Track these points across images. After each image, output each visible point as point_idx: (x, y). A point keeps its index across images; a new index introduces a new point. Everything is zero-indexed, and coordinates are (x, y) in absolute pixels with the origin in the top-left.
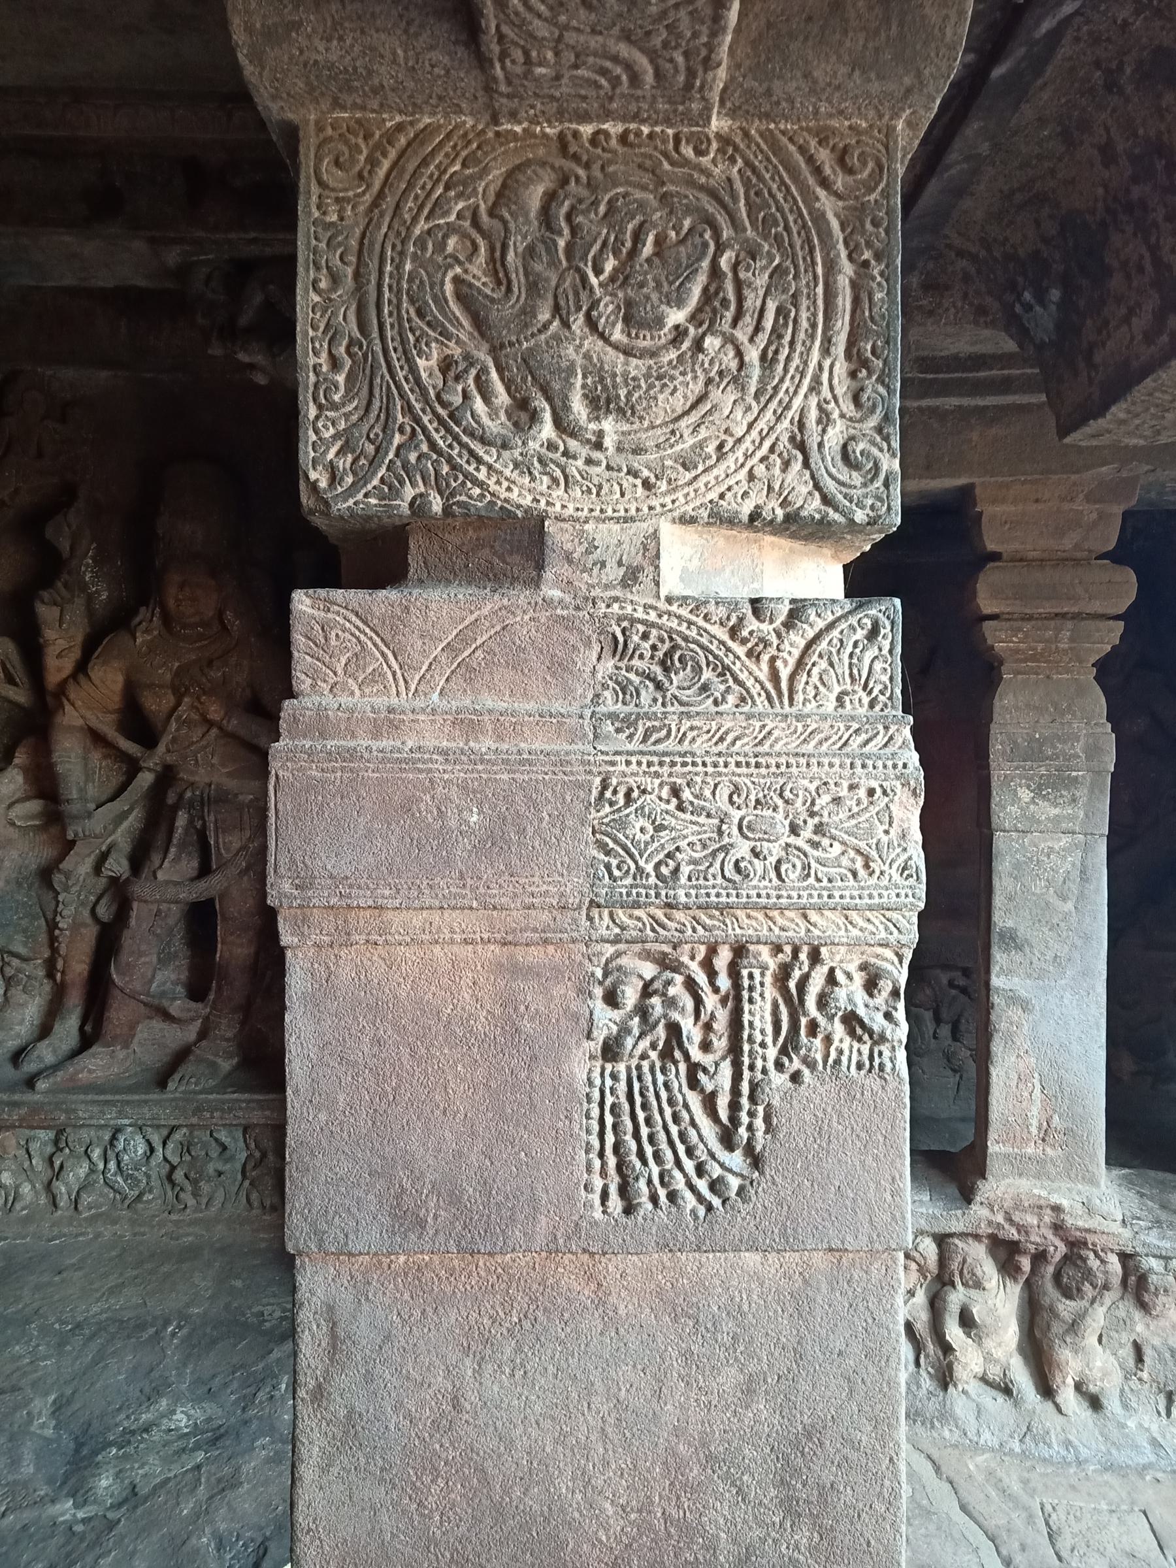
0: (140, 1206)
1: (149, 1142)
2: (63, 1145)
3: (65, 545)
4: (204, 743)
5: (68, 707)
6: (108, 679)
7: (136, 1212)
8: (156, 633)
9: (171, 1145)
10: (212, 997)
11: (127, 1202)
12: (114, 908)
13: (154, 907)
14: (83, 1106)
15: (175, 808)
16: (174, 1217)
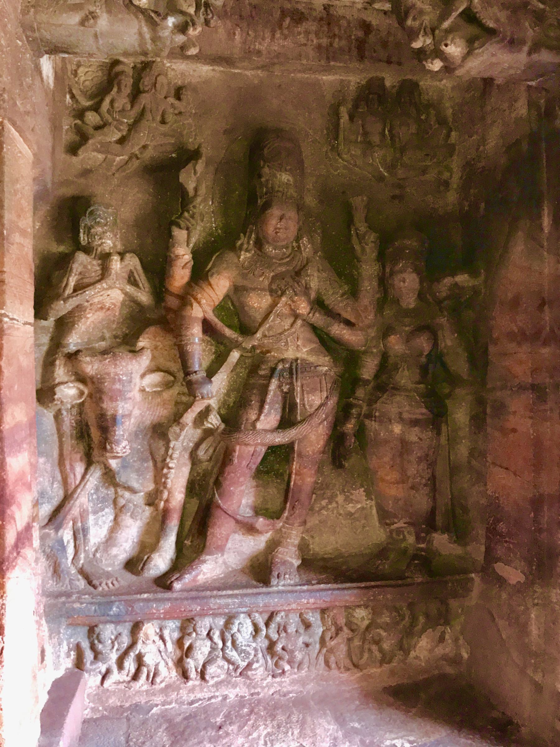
0: (250, 673)
3: (190, 186)
4: (293, 330)
5: (195, 304)
6: (221, 285)
7: (248, 677)
8: (253, 252)
9: (273, 626)
11: (239, 671)
13: (251, 449)
16: (278, 679)
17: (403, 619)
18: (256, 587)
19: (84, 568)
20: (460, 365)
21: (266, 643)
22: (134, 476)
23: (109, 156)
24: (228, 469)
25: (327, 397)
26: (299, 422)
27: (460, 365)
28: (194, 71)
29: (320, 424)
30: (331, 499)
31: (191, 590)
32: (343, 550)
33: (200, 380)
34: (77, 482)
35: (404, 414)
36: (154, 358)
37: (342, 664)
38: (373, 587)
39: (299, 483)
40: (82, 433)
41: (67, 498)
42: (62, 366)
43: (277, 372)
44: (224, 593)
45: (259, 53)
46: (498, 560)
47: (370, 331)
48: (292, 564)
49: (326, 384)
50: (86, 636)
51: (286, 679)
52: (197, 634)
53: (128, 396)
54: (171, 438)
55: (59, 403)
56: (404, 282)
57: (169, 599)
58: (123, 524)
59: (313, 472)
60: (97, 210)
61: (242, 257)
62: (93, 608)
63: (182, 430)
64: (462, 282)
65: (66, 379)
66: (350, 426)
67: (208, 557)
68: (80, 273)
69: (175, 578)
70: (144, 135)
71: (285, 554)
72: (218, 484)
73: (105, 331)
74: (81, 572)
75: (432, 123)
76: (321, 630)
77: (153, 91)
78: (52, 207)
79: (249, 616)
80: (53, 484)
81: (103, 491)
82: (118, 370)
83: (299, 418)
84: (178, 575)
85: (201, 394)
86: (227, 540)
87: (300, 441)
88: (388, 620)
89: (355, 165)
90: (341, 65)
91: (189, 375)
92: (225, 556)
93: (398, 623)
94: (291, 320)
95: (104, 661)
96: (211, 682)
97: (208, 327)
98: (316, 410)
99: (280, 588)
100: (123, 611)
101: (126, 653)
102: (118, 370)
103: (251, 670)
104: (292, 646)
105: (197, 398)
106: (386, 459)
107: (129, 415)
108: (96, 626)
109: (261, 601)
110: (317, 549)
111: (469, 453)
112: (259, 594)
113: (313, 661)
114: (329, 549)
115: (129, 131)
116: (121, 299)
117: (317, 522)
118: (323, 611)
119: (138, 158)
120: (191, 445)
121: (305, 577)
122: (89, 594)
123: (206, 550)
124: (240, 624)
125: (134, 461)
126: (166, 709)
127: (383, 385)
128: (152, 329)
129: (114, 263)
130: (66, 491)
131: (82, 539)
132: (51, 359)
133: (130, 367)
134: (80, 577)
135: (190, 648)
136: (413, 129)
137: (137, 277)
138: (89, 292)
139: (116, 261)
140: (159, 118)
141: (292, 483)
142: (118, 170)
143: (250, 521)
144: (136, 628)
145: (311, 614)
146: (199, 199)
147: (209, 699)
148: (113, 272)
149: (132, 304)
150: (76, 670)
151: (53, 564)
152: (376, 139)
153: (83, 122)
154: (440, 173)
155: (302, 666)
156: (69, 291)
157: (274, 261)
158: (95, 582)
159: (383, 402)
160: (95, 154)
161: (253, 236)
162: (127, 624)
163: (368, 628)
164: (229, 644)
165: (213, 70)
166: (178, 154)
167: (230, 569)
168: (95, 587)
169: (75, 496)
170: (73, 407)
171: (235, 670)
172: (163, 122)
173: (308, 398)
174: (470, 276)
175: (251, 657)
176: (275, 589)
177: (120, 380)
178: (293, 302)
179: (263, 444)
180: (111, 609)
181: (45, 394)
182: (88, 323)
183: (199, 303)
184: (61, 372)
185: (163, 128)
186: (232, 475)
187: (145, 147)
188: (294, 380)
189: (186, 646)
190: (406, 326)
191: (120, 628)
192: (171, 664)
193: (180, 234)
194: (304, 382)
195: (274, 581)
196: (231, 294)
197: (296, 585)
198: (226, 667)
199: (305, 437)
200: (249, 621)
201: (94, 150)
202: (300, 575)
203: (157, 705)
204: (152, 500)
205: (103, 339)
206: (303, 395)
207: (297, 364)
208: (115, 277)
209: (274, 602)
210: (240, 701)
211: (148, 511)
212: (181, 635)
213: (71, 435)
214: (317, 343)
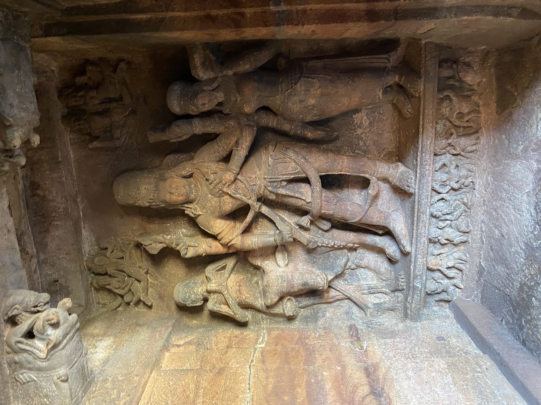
1: (438, 201)
3: (161, 246)
5: (233, 242)
6: (219, 226)
8: (196, 206)
9: (440, 190)
10: (367, 176)
11: (467, 210)
12: (325, 222)
13: (324, 203)
14: (419, 231)
15: (277, 195)
16: (477, 188)
20: (264, 57)
21: (451, 191)
23: (149, 285)
28: (87, 239)
30: (359, 138)
33: (280, 238)
37: (474, 141)
38: (423, 123)
41: (349, 299)
45: (66, 209)
51: (478, 181)
57: (416, 256)
58: (367, 265)
61: (200, 213)
63: (311, 242)
67: (391, 225)
74: (393, 291)
80: (341, 306)
86: (382, 212)
87: (319, 172)
90: (59, 153)
93: (451, 100)
95: (448, 287)
96: (472, 228)
97: (247, 230)
99: (417, 187)
101: (445, 275)
103: (468, 203)
104: (456, 178)
110: (393, 146)
112: (419, 202)
113: (468, 161)
117: (374, 147)
118: (436, 155)
120: (320, 231)
126: (484, 257)
134: (396, 293)
135: (447, 240)
137: (219, 267)
139: (210, 286)
141: (347, 173)
143: (370, 197)
147: (482, 231)
149: (236, 267)
150: (451, 303)
153: (131, 301)
155: (471, 170)
158: (400, 288)
164: (448, 217)
165: (84, 228)
169: (349, 295)
170: (297, 301)
171: (465, 211)
172: (122, 258)
174: (195, 53)
175: (459, 203)
177: (281, 283)
180: (418, 287)
181: (290, 319)
183: (232, 240)
184: (278, 310)
187: (140, 268)
188: (279, 180)
189: (447, 242)
190: (237, 100)
192: (456, 249)
193: (190, 253)
195: (412, 191)
197: (416, 176)
198: (463, 217)
200: (435, 205)
201: (147, 294)
203: (480, 262)
204: (353, 249)
205: (257, 283)
210: (488, 213)
211: (360, 251)
212: (438, 244)
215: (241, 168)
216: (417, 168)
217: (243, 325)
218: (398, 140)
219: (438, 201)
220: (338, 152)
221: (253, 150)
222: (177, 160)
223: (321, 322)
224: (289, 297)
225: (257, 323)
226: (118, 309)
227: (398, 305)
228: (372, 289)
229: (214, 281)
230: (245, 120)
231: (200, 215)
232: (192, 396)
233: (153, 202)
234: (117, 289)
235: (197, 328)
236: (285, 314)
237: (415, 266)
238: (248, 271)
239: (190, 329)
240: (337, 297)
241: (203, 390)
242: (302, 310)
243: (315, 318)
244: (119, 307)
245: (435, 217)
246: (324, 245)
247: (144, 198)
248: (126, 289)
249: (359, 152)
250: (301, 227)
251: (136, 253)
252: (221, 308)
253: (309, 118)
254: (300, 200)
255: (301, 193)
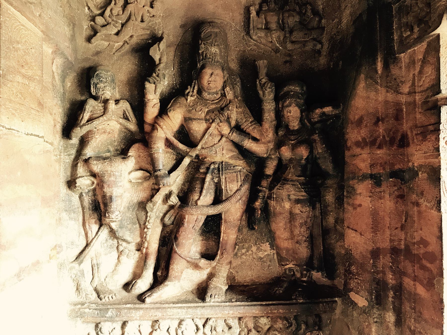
1: (197, 326)
2: (157, 327)
3: (157, 59)
4: (220, 144)
5: (159, 129)
6: (175, 118)
8: (196, 97)
9: (208, 327)
10: (218, 257)
12: (173, 218)
13: (195, 218)
15: (206, 173)
17: (291, 326)
18: (197, 302)
19: (97, 287)
22: (128, 233)
24: (181, 229)
25: (241, 185)
26: (224, 201)
27: (327, 166)
29: (237, 202)
31: (157, 303)
32: (257, 280)
34: (93, 237)
35: (291, 196)
36: (137, 162)
39: (226, 238)
40: (96, 206)
41: (87, 245)
42: (82, 167)
43: (210, 170)
44: (177, 305)
46: (351, 290)
47: (269, 144)
48: (221, 289)
49: (241, 178)
50: (94, 328)
52: (160, 330)
53: (119, 185)
54: (148, 210)
55: (79, 189)
56: (290, 113)
57: (142, 309)
59: (234, 232)
60: (101, 73)
61: (189, 100)
62: (97, 312)
63: (154, 205)
64: (328, 111)
65: (84, 175)
66: (258, 204)
68: (91, 111)
69: (148, 295)
70: (131, 29)
71: (217, 282)
72: (176, 238)
73: (110, 147)
74: (96, 290)
75: (309, 14)
76: (238, 330)
77: (136, 2)
78: (77, 74)
79: (193, 320)
81: (110, 242)
82: (113, 169)
83: (224, 198)
84: (150, 293)
85: (163, 183)
86: (182, 273)
88: (281, 326)
89: (261, 43)
91: (156, 172)
92: (181, 281)
93: (288, 328)
94: (220, 137)
98: (234, 193)
99: (212, 304)
100: (115, 314)
102: (113, 169)
105: (160, 186)
106: (281, 224)
107: (121, 196)
108: (99, 323)
109: (199, 312)
110: (240, 280)
111: (335, 221)
112: (198, 307)
114: (248, 279)
115: (122, 27)
116: (118, 127)
117: (240, 263)
118: (240, 319)
119: (128, 44)
120: (161, 215)
121: (229, 297)
122: (95, 304)
123: (169, 279)
124: (186, 325)
125: (128, 224)
127: (279, 178)
128: (136, 146)
129: (110, 104)
130: (87, 241)
131: (97, 269)
132: (75, 163)
133: (120, 167)
136: (297, 19)
138: (96, 122)
140: (140, 19)
141: (221, 239)
142: (116, 51)
143: (196, 261)
144: (124, 324)
145: (231, 320)
146: (162, 65)
148: (110, 110)
151: (76, 285)
152: (273, 26)
154: (315, 45)
156: (84, 121)
157: (208, 101)
158: (102, 296)
159: (278, 189)
160: (103, 42)
161: (196, 87)
162: (119, 322)
163: (269, 329)
166: (152, 41)
167: (185, 291)
168: (101, 299)
169: (92, 244)
170: (89, 191)
172: (142, 21)
173: (229, 186)
174: (333, 108)
176: (208, 304)
177: (114, 175)
178: (219, 126)
179: (202, 214)
181: (71, 184)
182: (97, 141)
183: (162, 128)
184: (81, 170)
185: (144, 25)
186: (184, 233)
187: (131, 36)
188: (221, 175)
190: (292, 140)
191: (115, 325)
193: (149, 87)
194: (227, 176)
195: (208, 299)
196: (183, 123)
199: (228, 210)
201: (102, 40)
202: (226, 295)
205: (109, 151)
206: (226, 184)
207: (222, 165)
208: (111, 113)
209: (207, 313)
211: (137, 254)
212: (151, 330)
213: (89, 208)
214: (236, 152)
215: (232, 141)
216: (229, 302)
217: (67, 133)
218: (245, 284)
219: (197, 326)
220: (240, 230)
221: (244, 153)
222: (236, 84)
223: (64, 215)
224: (95, 182)
225: (66, 148)
226: (86, 8)
227: (84, 296)
228: (98, 268)
229: (116, 107)
230: (272, 147)
231: (187, 100)
232: (23, 71)
233: (202, 56)
234: (111, 10)
235: (63, 86)
236: (77, 178)
237: (130, 308)
238: (121, 142)
239: (63, 79)
240: (89, 232)
241: (28, 84)
242: (77, 197)
243: (69, 210)
244: (89, 8)
245: (180, 324)
246: (148, 218)
247: (207, 49)
248: (110, 20)
249: (236, 249)
250: (168, 197)
251: (147, 34)
252: (88, 112)
253: (272, 203)
254: (199, 194)
255: (206, 196)
